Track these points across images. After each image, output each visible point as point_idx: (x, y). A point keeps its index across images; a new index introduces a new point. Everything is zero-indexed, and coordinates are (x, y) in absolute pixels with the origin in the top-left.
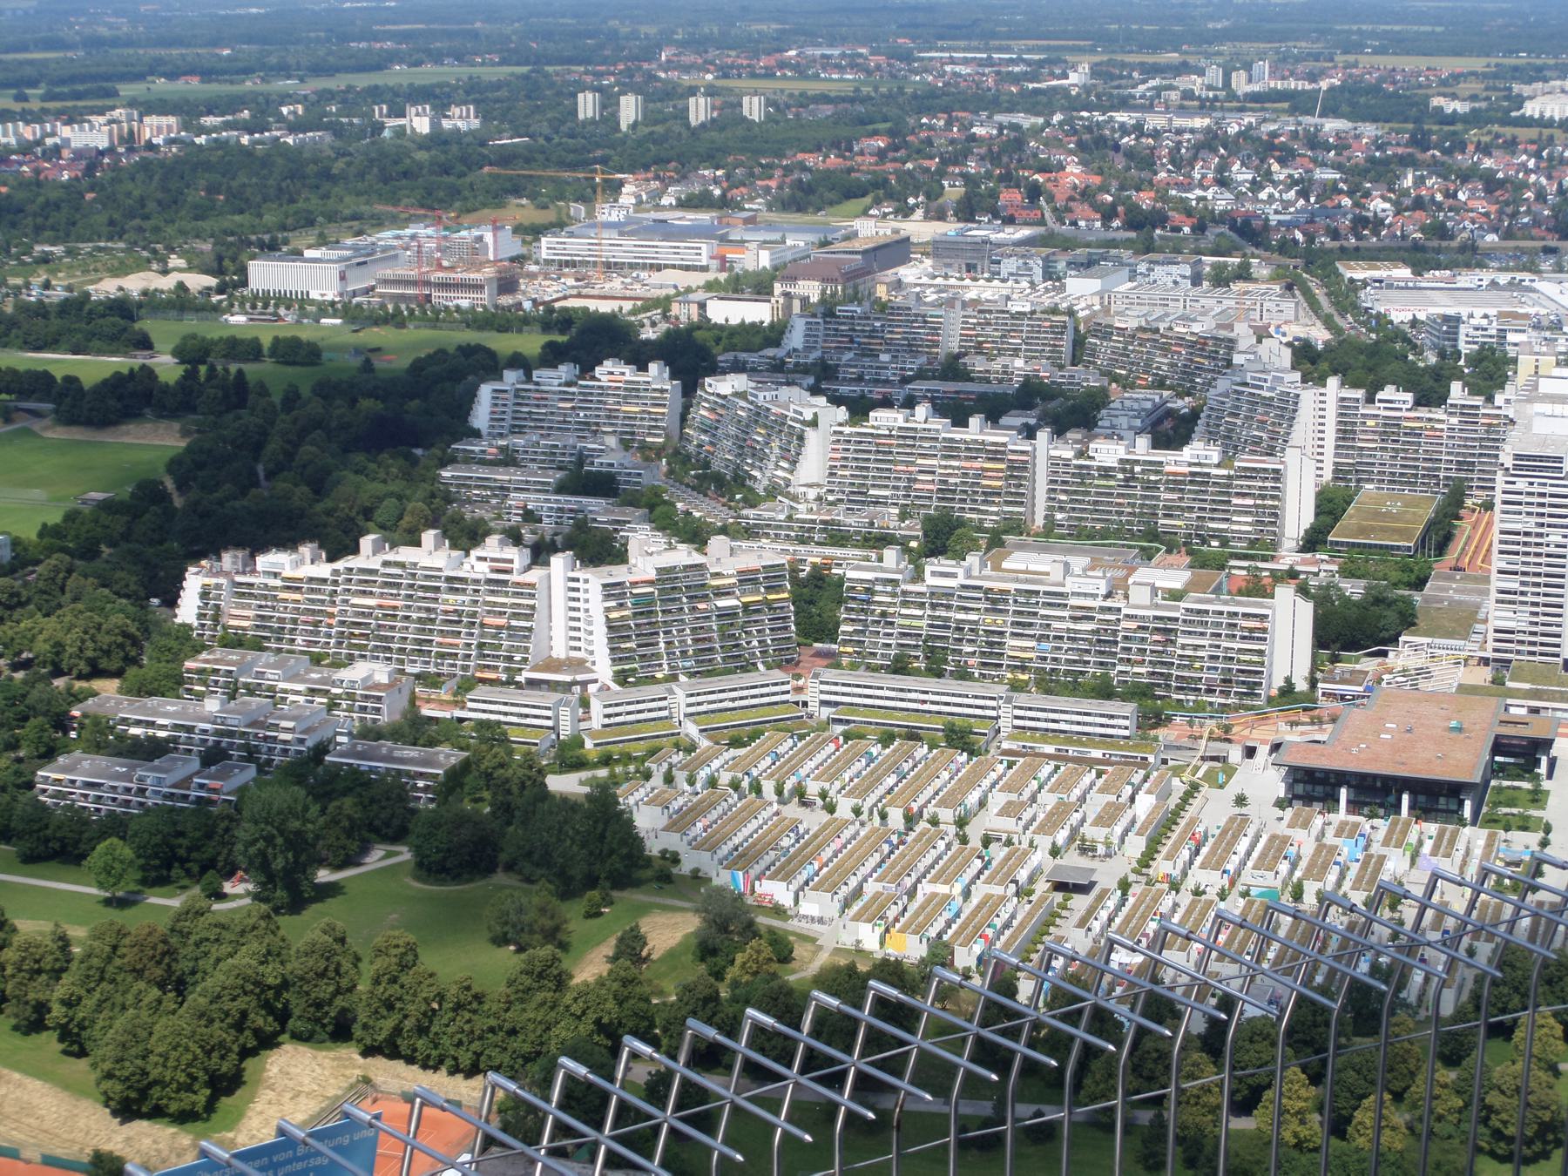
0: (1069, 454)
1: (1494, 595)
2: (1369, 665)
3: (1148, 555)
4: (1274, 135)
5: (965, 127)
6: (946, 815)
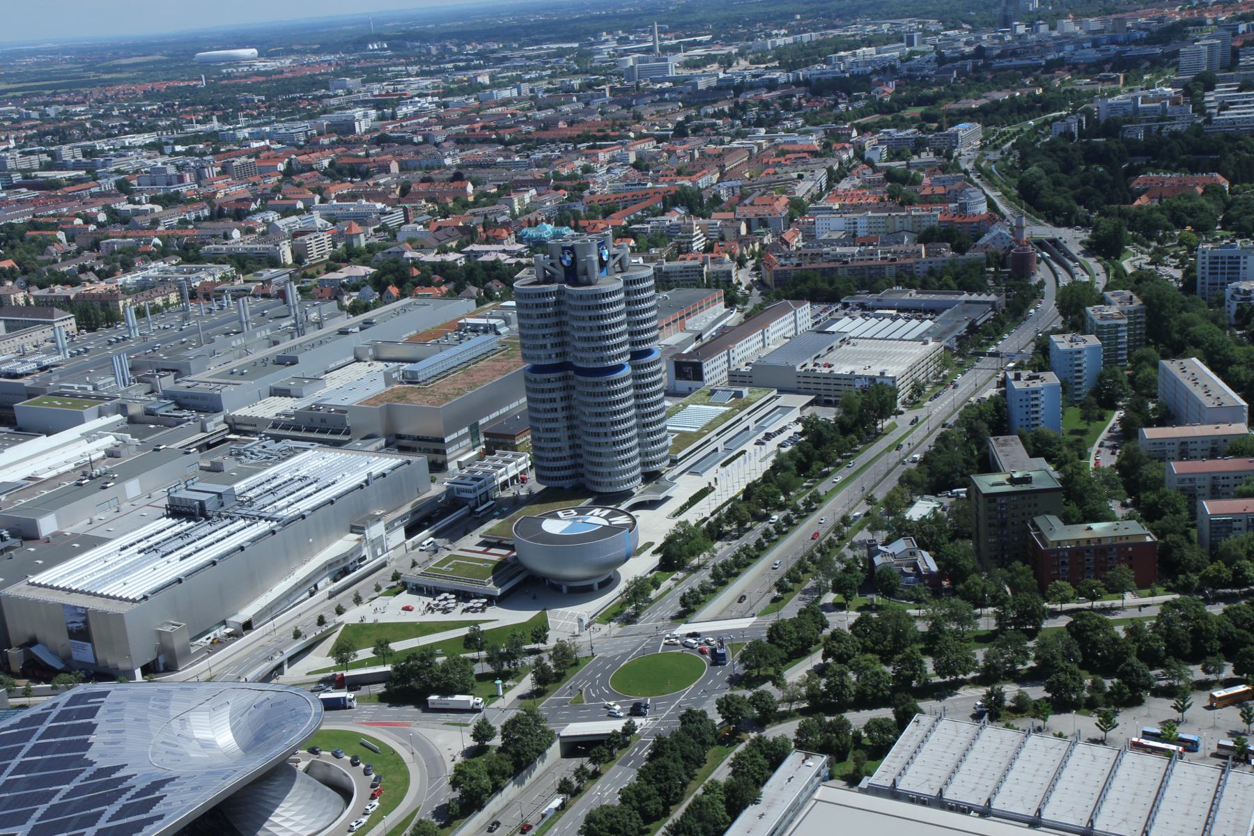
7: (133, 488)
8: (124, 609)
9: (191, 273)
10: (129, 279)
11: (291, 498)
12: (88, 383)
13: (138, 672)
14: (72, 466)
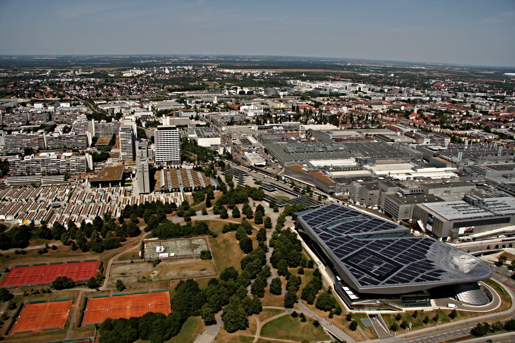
0: (49, 136)
1: (121, 151)
2: (103, 164)
3: (65, 151)
4: (83, 81)
5: (28, 82)
6: (33, 199)
7: (455, 189)
8: (444, 221)
9: (486, 135)
10: (468, 132)
11: (500, 209)
12: (450, 157)
13: (441, 239)
14: (440, 178)
